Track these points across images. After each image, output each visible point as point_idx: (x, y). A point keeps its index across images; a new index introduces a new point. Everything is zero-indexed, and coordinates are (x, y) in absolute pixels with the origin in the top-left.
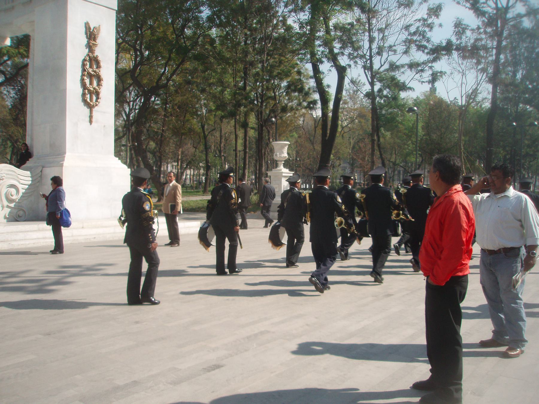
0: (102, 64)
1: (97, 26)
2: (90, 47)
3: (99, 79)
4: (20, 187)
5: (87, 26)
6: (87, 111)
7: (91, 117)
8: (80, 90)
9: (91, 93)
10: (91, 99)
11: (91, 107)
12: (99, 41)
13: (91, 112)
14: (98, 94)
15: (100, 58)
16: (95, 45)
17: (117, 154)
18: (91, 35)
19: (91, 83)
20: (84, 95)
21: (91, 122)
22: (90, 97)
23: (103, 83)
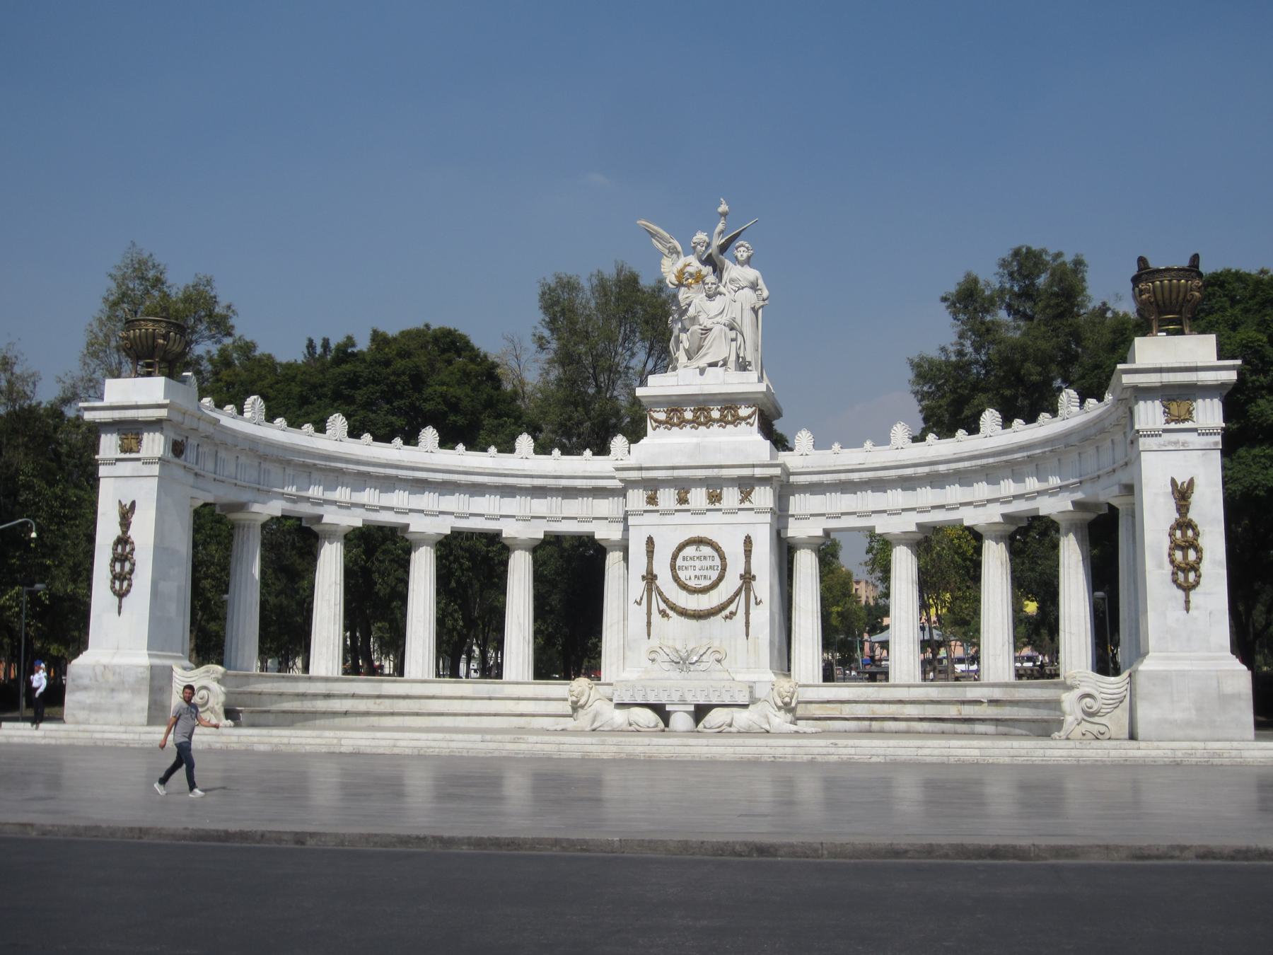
0: (1200, 528)
1: (1187, 479)
3: (1198, 550)
5: (1173, 482)
6: (1180, 593)
7: (1187, 602)
8: (1169, 568)
9: (1183, 570)
11: (1187, 588)
12: (1195, 499)
13: (1187, 596)
18: (1182, 495)
19: (1185, 556)
20: (1174, 574)
21: (1187, 609)
22: (1186, 576)
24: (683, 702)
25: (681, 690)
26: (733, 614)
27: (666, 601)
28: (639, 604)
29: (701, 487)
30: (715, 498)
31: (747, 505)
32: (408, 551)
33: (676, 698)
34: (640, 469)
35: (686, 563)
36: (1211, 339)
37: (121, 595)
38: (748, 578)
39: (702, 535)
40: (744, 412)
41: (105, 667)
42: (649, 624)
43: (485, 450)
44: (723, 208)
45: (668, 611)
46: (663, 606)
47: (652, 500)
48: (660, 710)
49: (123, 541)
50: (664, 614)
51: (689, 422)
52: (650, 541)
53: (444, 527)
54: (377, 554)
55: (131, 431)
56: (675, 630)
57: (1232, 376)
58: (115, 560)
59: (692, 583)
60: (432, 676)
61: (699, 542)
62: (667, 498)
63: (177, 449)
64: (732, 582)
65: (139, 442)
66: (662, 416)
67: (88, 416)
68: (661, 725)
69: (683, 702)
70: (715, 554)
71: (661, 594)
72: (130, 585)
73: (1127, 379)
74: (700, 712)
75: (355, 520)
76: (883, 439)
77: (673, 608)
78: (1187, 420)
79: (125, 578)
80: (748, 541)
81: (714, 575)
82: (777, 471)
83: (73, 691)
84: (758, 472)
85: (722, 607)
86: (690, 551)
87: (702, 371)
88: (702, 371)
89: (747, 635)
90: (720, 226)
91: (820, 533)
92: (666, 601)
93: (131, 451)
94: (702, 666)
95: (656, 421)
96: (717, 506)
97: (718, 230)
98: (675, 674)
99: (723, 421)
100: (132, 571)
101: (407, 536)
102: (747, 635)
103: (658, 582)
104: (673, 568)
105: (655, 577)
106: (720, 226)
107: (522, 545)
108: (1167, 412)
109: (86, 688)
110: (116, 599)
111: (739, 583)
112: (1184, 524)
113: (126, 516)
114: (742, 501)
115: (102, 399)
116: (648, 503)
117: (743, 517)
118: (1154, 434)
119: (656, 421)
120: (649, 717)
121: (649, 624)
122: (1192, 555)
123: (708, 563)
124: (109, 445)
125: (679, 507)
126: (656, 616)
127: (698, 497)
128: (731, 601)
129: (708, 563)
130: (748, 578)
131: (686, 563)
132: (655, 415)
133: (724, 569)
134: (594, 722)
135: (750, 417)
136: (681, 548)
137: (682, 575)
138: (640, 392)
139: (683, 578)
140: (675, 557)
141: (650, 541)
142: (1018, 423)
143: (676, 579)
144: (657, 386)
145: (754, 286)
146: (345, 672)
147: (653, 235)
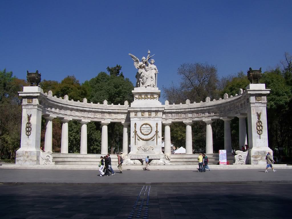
0: (262, 122)
2: (259, 118)
3: (262, 127)
4: (242, 156)
7: (260, 137)
9: (259, 130)
10: (260, 133)
12: (261, 117)
13: (260, 136)
14: (262, 131)
15: (262, 121)
16: (260, 118)
17: (269, 146)
18: (259, 116)
21: (260, 139)
22: (259, 132)
23: (263, 127)
25: (144, 156)
27: (139, 137)
29: (147, 112)
32: (82, 125)
34: (134, 108)
35: (143, 129)
36: (264, 85)
37: (28, 135)
38: (157, 132)
39: (147, 123)
40: (155, 96)
41: (26, 151)
42: (135, 142)
43: (97, 103)
44: (149, 52)
45: (140, 139)
46: (138, 138)
47: (136, 115)
49: (29, 123)
50: (138, 140)
51: (143, 98)
52: (135, 124)
53: (89, 121)
54: (75, 126)
55: (30, 98)
56: (141, 143)
57: (268, 92)
58: (27, 127)
59: (145, 133)
60: (87, 153)
61: (146, 124)
62: (139, 114)
63: (40, 102)
64: (154, 133)
65: (32, 101)
66: (137, 97)
67: (20, 95)
68: (141, 164)
70: (150, 127)
72: (31, 133)
73: (249, 92)
74: (150, 160)
75: (71, 118)
76: (184, 103)
77: (141, 139)
78: (260, 101)
79: (30, 132)
81: (150, 131)
82: (164, 109)
83: (18, 157)
84: (160, 109)
85: (152, 138)
86: (144, 126)
87: (146, 87)
88: (146, 87)
89: (157, 144)
90: (148, 56)
91: (171, 123)
92: (139, 137)
93: (30, 103)
94: (150, 151)
95: (136, 98)
97: (148, 57)
98: (143, 152)
99: (151, 98)
100: (31, 130)
101: (81, 122)
102: (157, 144)
103: (137, 133)
104: (140, 130)
106: (148, 56)
107: (105, 124)
108: (256, 99)
109: (21, 156)
110: (27, 136)
112: (259, 122)
113: (29, 117)
114: (156, 115)
115: (23, 91)
117: (156, 119)
118: (254, 103)
120: (139, 162)
121: (135, 142)
122: (261, 128)
124: (25, 102)
127: (147, 114)
128: (153, 137)
130: (157, 132)
131: (143, 129)
132: (136, 97)
133: (152, 130)
134: (126, 163)
136: (142, 125)
137: (142, 131)
138: (133, 91)
139: (143, 132)
140: (141, 127)
141: (135, 124)
142: (214, 100)
143: (141, 132)
144: (136, 90)
145: (155, 69)
146: (69, 152)
147: (132, 57)
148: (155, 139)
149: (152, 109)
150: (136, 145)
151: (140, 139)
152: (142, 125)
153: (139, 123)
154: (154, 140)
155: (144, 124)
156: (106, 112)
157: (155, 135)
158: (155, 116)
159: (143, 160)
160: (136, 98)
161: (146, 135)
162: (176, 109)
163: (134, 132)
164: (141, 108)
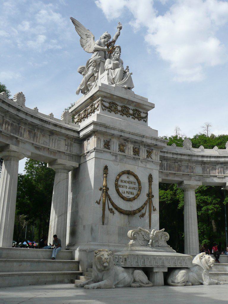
24: (163, 267)
26: (143, 216)
27: (113, 204)
28: (98, 203)
30: (136, 152)
31: (149, 159)
33: (160, 263)
38: (150, 196)
39: (131, 170)
45: (114, 209)
46: (111, 207)
48: (148, 271)
50: (111, 211)
51: (119, 111)
52: (106, 168)
59: (125, 195)
64: (143, 198)
69: (163, 267)
70: (135, 180)
71: (110, 199)
77: (117, 208)
80: (150, 178)
81: (135, 192)
85: (139, 210)
86: (124, 177)
96: (137, 157)
103: (109, 192)
105: (107, 189)
111: (146, 198)
116: (105, 147)
117: (149, 166)
119: (105, 106)
120: (140, 275)
123: (132, 186)
125: (120, 153)
126: (107, 212)
129: (132, 186)
130: (150, 196)
132: (105, 103)
135: (145, 118)
136: (120, 175)
137: (121, 190)
139: (121, 191)
140: (117, 180)
141: (106, 168)
148: (147, 214)
149: (144, 140)
150: (105, 226)
151: (115, 211)
152: (120, 175)
153: (115, 169)
154: (145, 214)
155: (124, 173)
156: (26, 123)
157: (145, 204)
158: (146, 157)
159: (154, 271)
160: (104, 108)
161: (129, 200)
162: (173, 153)
163: (101, 189)
164: (122, 131)
